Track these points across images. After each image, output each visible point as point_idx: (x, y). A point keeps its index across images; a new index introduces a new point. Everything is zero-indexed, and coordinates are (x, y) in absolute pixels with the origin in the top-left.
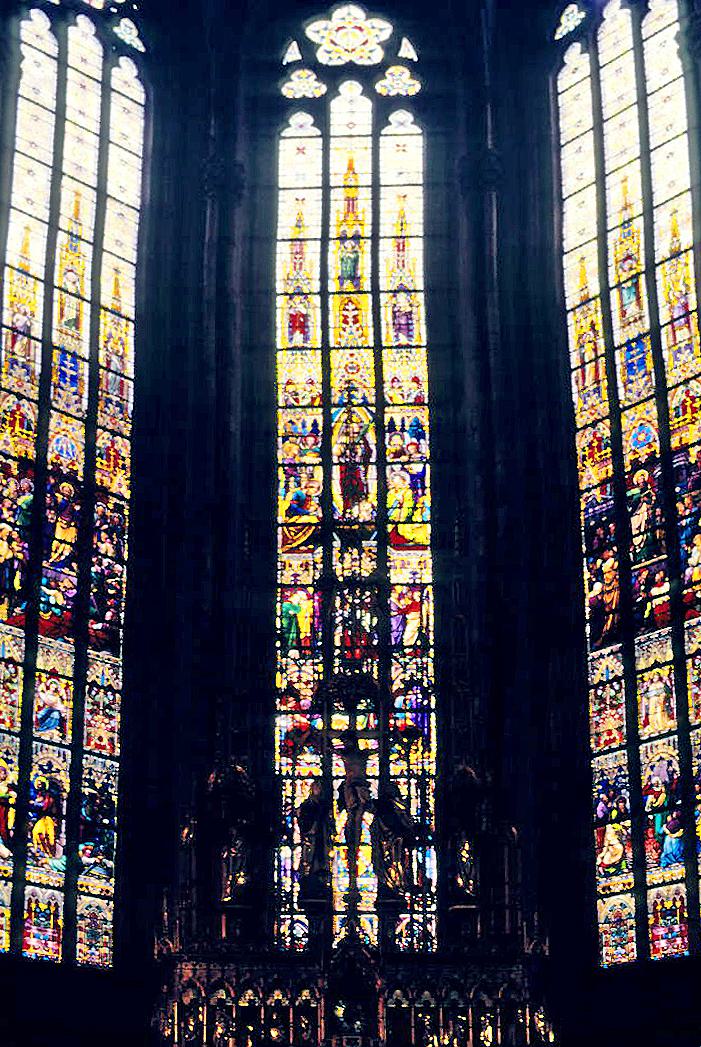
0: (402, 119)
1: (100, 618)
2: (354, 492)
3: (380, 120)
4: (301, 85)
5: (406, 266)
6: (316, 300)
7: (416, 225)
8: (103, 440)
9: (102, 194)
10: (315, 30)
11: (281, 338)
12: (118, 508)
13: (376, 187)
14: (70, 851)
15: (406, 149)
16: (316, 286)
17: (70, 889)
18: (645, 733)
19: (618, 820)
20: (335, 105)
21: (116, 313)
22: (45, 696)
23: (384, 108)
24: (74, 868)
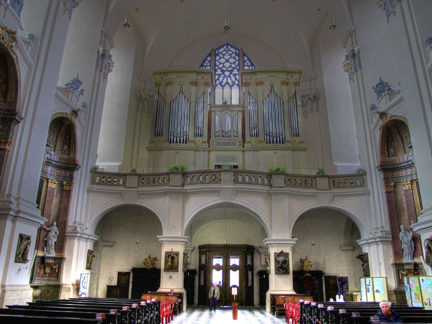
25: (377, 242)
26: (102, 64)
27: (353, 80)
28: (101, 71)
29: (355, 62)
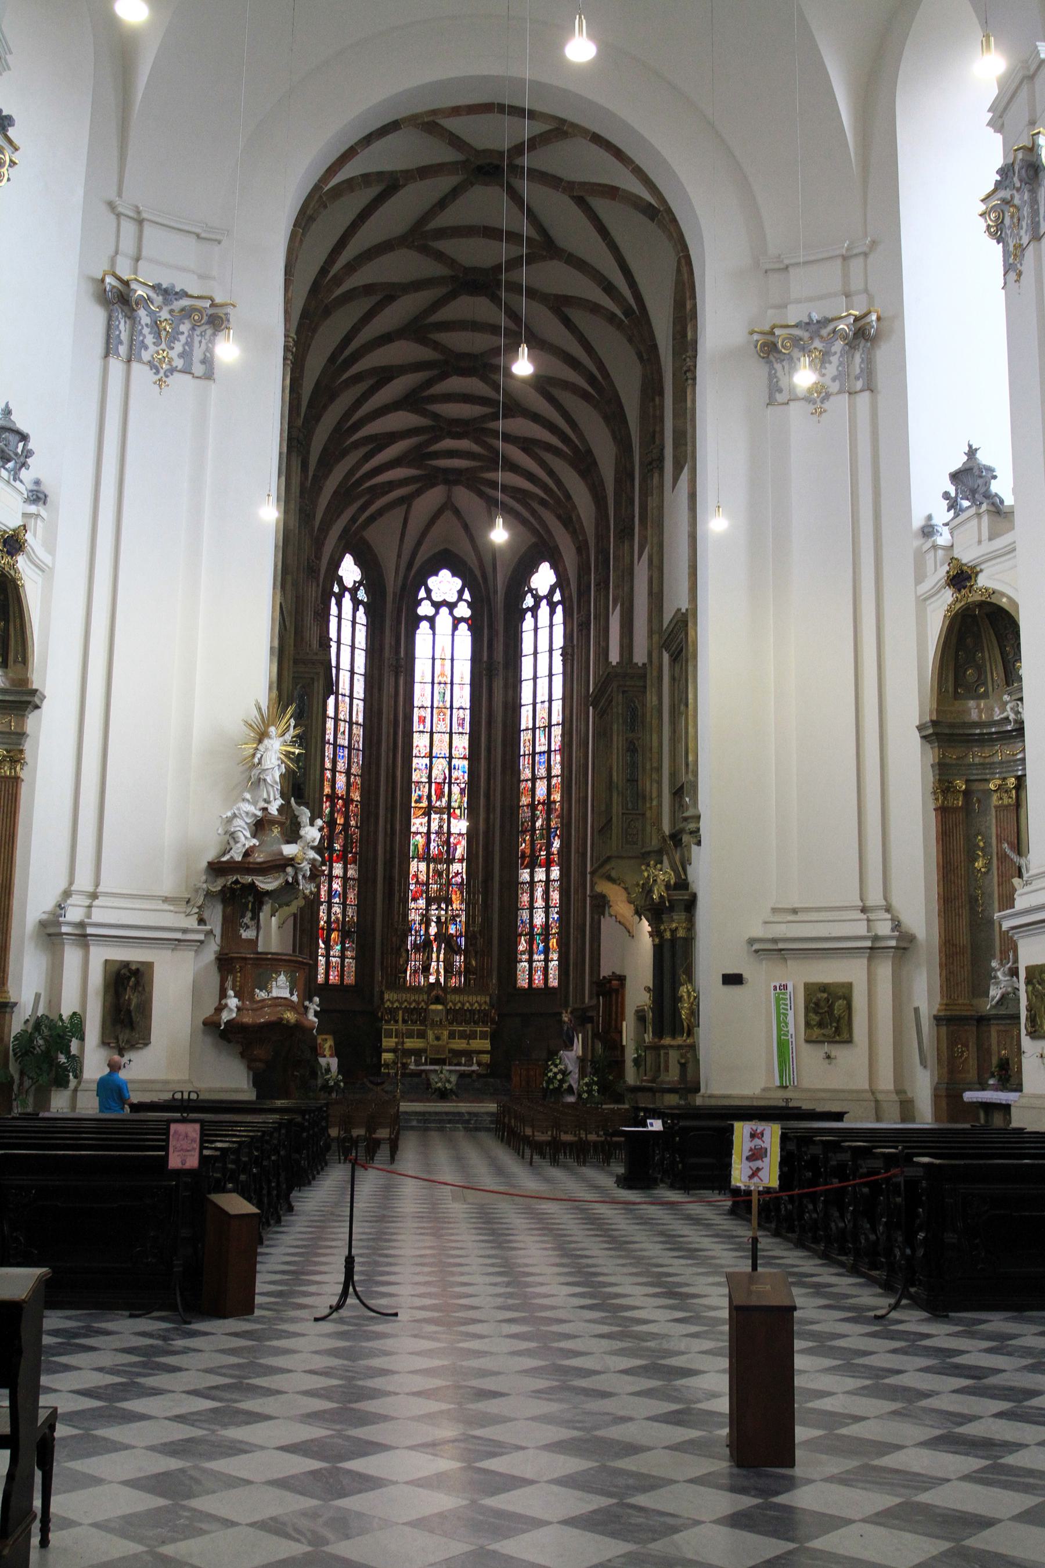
0: (463, 627)
1: (351, 852)
2: (440, 795)
3: (455, 628)
4: (425, 609)
5: (463, 697)
6: (429, 710)
7: (467, 679)
8: (352, 780)
9: (352, 672)
10: (432, 582)
11: (416, 727)
12: (357, 806)
13: (452, 660)
14: (343, 943)
16: (429, 705)
17: (343, 957)
18: (536, 905)
19: (526, 935)
20: (438, 618)
21: (357, 723)
22: (335, 886)
23: (457, 622)
24: (343, 950)
29: (1034, 202)
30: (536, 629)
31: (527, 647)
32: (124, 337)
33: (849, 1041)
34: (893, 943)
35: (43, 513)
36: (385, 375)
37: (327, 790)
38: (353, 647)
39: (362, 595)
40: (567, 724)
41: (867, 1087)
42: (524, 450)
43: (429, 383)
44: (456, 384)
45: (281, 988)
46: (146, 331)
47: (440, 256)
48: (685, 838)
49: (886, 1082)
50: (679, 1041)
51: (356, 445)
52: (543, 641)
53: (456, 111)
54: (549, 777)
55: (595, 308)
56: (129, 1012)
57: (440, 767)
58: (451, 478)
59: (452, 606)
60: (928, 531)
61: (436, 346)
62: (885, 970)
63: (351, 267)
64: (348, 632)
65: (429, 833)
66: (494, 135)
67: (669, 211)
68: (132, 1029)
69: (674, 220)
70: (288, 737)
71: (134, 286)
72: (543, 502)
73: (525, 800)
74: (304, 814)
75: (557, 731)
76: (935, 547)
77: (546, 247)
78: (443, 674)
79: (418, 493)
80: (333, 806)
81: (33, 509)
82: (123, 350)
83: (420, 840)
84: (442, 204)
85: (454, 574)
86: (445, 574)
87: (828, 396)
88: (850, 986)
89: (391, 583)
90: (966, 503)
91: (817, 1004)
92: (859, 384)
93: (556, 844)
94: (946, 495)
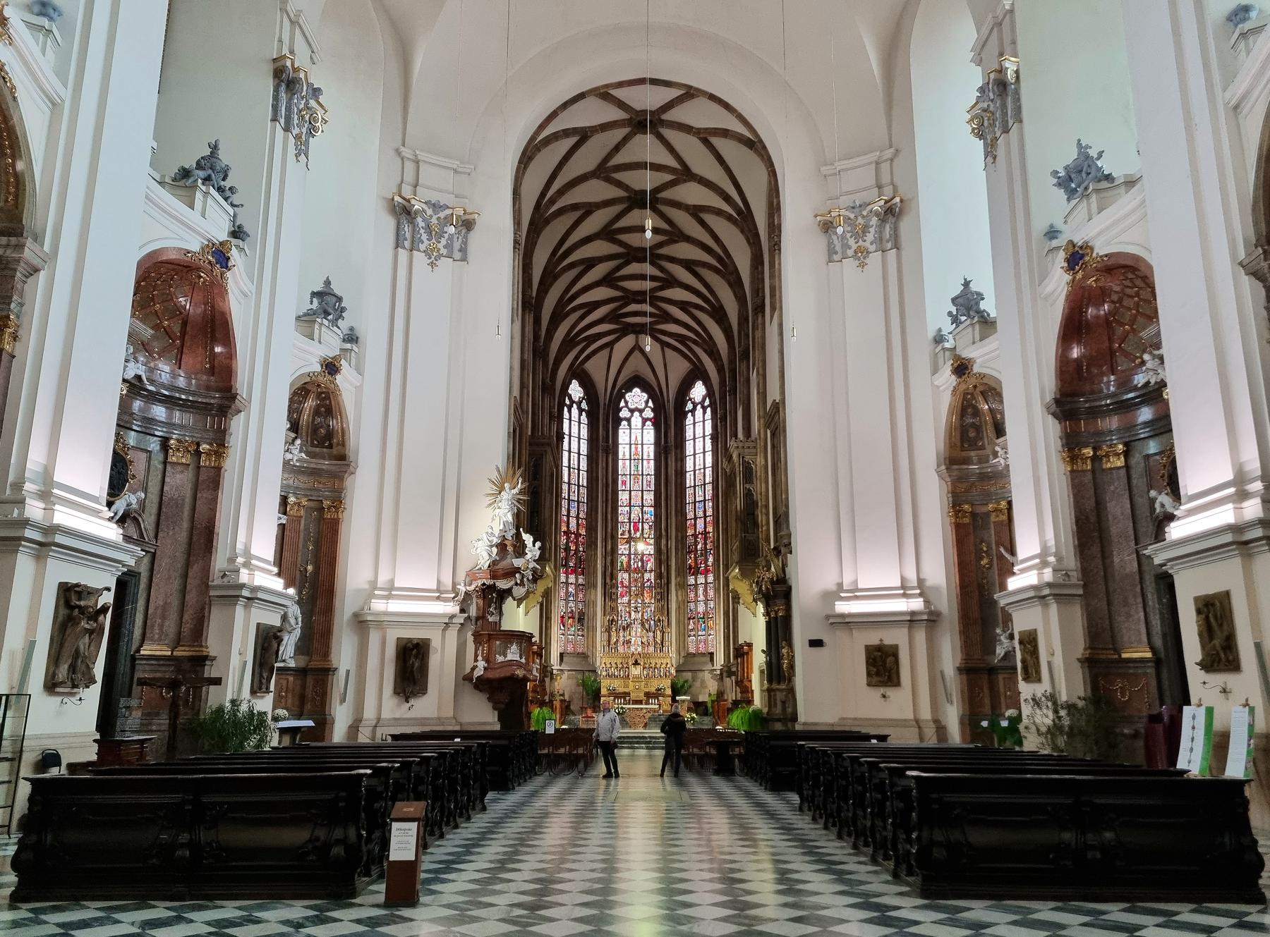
0: (649, 423)
2: (636, 530)
3: (644, 424)
4: (624, 413)
5: (650, 467)
7: (652, 456)
9: (579, 454)
10: (628, 396)
15: (650, 435)
23: (644, 421)
25: (1044, 597)
26: (289, 109)
27: (995, 158)
28: (287, 129)
29: (1004, 106)
30: (694, 424)
31: (689, 433)
32: (408, 235)
33: (898, 684)
34: (925, 617)
35: (355, 348)
36: (590, 264)
37: (564, 528)
38: (579, 439)
39: (584, 405)
40: (715, 482)
41: (911, 717)
42: (682, 309)
43: (618, 268)
44: (634, 268)
45: (513, 654)
46: (422, 231)
47: (619, 184)
48: (783, 550)
49: (926, 714)
50: (783, 686)
51: (574, 309)
52: (699, 429)
53: (620, 85)
54: (705, 517)
55: (719, 212)
56: (412, 672)
57: (636, 512)
58: (639, 330)
59: (641, 411)
60: (939, 339)
61: (621, 243)
62: (921, 636)
63: (561, 192)
64: (575, 428)
65: (629, 555)
66: (648, 99)
67: (761, 141)
68: (415, 683)
69: (764, 147)
70: (516, 491)
71: (413, 202)
72: (695, 342)
73: (690, 532)
74: (528, 538)
75: (709, 488)
76: (944, 349)
77: (685, 174)
78: (636, 454)
79: (617, 340)
80: (568, 538)
81: (348, 346)
82: (407, 244)
83: (624, 559)
84: (617, 148)
85: (643, 390)
86: (637, 390)
87: (868, 253)
88: (896, 647)
89: (603, 399)
90: (963, 318)
91: (874, 660)
92: (889, 245)
93: (711, 559)
94: (950, 314)
